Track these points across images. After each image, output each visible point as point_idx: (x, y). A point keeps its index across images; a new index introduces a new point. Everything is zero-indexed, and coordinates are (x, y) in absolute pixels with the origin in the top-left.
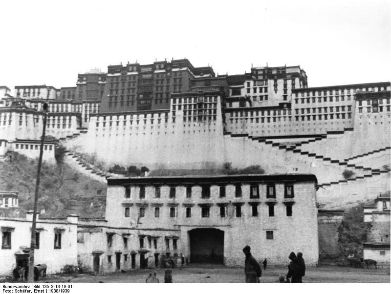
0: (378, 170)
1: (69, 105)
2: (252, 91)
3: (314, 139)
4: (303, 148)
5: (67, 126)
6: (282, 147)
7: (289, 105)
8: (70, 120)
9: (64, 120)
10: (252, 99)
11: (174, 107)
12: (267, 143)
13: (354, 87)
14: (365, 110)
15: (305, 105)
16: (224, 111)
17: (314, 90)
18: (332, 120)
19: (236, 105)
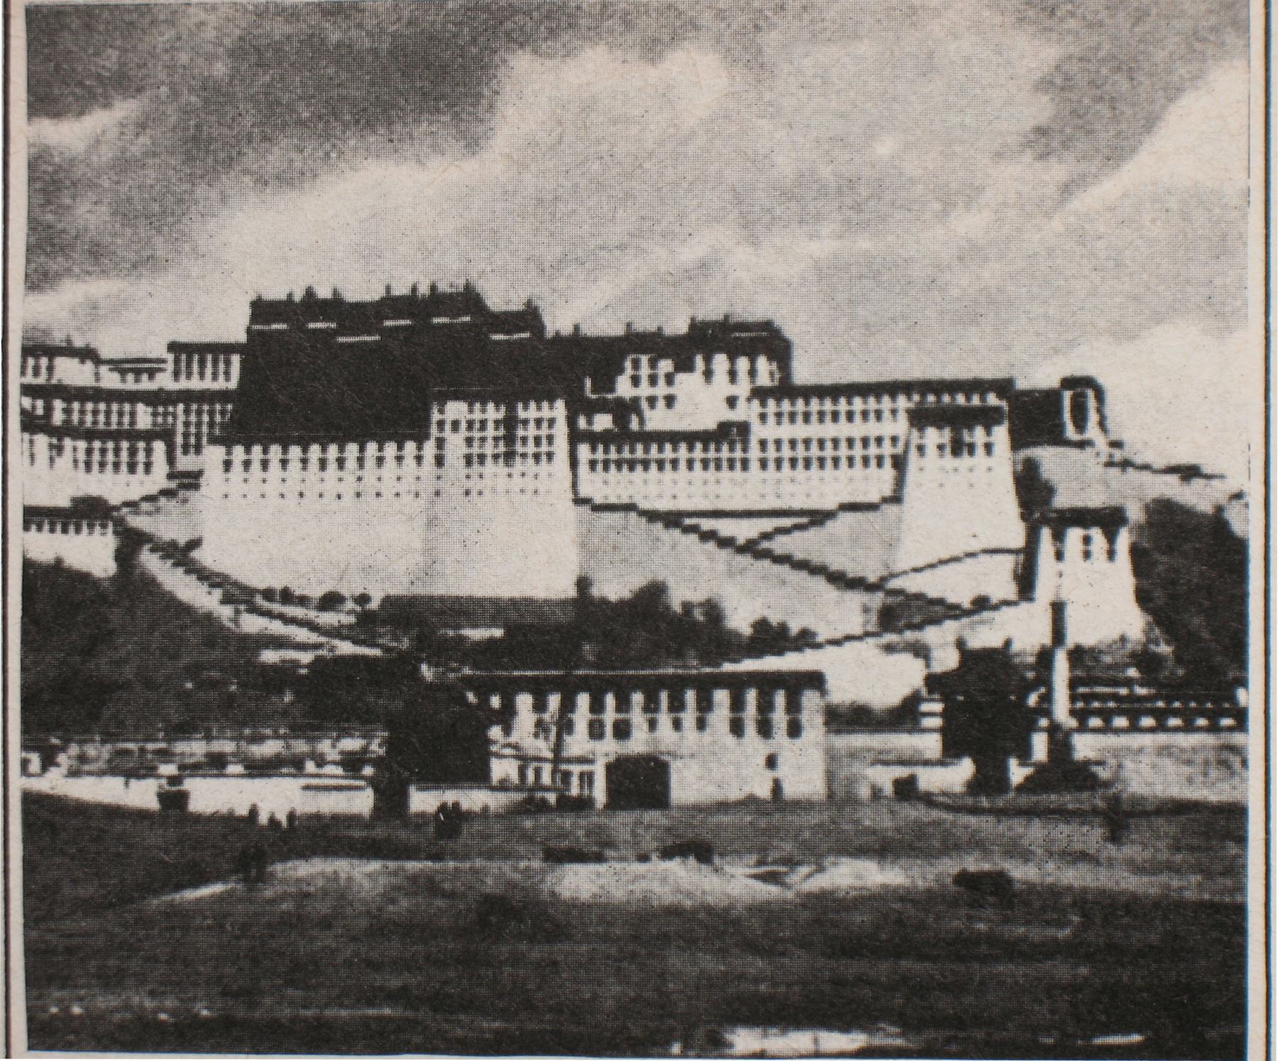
0: (955, 607)
1: (141, 408)
2: (644, 381)
3: (804, 520)
4: (780, 545)
5: (141, 468)
6: (726, 543)
7: (744, 428)
8: (149, 451)
9: (133, 452)
10: (644, 405)
11: (441, 424)
12: (688, 530)
13: (906, 387)
14: (931, 450)
15: (786, 431)
16: (575, 437)
17: (808, 392)
18: (850, 472)
19: (603, 422)
